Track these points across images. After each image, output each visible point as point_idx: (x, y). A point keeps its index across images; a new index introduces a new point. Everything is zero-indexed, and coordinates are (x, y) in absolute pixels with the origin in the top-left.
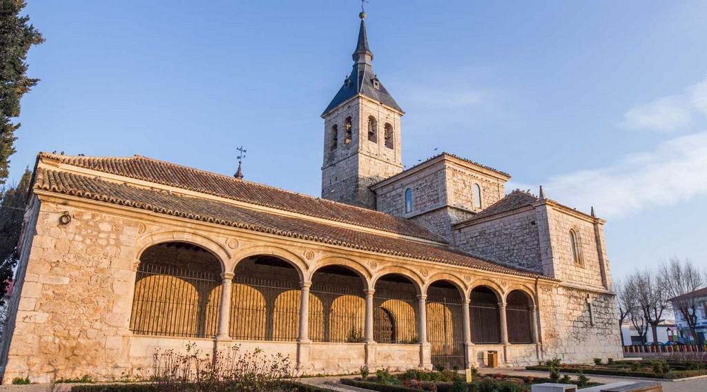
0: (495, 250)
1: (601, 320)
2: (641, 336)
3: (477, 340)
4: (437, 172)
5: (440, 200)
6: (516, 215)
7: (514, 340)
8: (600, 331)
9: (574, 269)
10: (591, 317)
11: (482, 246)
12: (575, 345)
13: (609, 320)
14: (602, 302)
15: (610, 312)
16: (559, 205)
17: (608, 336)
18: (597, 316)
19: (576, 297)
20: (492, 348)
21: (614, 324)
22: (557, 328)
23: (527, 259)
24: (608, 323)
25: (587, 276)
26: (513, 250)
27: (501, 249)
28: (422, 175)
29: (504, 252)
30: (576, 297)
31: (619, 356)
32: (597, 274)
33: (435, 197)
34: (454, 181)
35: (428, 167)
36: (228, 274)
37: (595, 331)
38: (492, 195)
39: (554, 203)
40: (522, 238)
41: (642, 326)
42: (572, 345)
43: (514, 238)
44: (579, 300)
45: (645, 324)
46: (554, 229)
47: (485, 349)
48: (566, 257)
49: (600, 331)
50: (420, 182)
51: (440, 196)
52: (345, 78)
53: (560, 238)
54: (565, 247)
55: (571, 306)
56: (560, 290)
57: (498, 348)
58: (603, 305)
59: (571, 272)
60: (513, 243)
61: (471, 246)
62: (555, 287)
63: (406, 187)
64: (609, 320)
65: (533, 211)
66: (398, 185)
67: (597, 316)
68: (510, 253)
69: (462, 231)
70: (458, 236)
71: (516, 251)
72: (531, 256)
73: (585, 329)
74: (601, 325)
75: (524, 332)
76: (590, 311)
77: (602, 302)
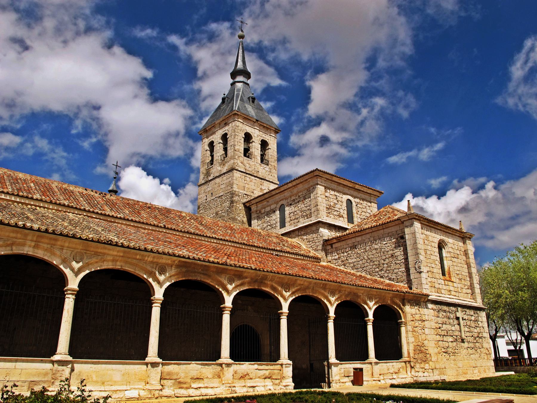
0: (365, 265)
1: (471, 334)
2: (516, 350)
3: (342, 357)
4: (309, 188)
5: (312, 215)
6: (385, 230)
7: (381, 356)
8: (471, 345)
9: (443, 283)
10: (460, 331)
11: (353, 260)
12: (445, 360)
13: (479, 333)
14: (472, 316)
15: (481, 325)
16: (427, 219)
17: (479, 350)
18: (466, 329)
19: (445, 311)
20: (358, 365)
21: (485, 337)
22: (426, 342)
23: (396, 273)
24: (478, 337)
25: (456, 289)
26: (383, 264)
27: (371, 264)
28: (295, 190)
29: (374, 266)
30: (445, 311)
31: (491, 373)
32: (466, 287)
33: (308, 212)
34: (326, 197)
35: (301, 182)
36: (285, 313)
37: (466, 345)
38: (365, 210)
39: (422, 217)
40: (391, 252)
41: (516, 340)
42: (442, 360)
43: (384, 253)
44: (448, 314)
45: (519, 338)
46: (423, 243)
47: (350, 366)
48: (435, 270)
49: (471, 345)
50: (293, 198)
51: (313, 210)
52: (223, 96)
53: (428, 252)
54: (434, 261)
55: (440, 320)
56: (430, 306)
57: (365, 367)
58: (473, 318)
59: (440, 286)
60: (384, 257)
61: (342, 261)
62: (423, 302)
63: (280, 204)
64: (479, 333)
65: (401, 225)
66: (271, 200)
67: (466, 329)
68: (380, 268)
69: (334, 246)
70: (330, 251)
71: (385, 265)
72: (400, 270)
73: (455, 343)
74: (471, 339)
75: (390, 350)
76: (459, 324)
77: (472, 316)
